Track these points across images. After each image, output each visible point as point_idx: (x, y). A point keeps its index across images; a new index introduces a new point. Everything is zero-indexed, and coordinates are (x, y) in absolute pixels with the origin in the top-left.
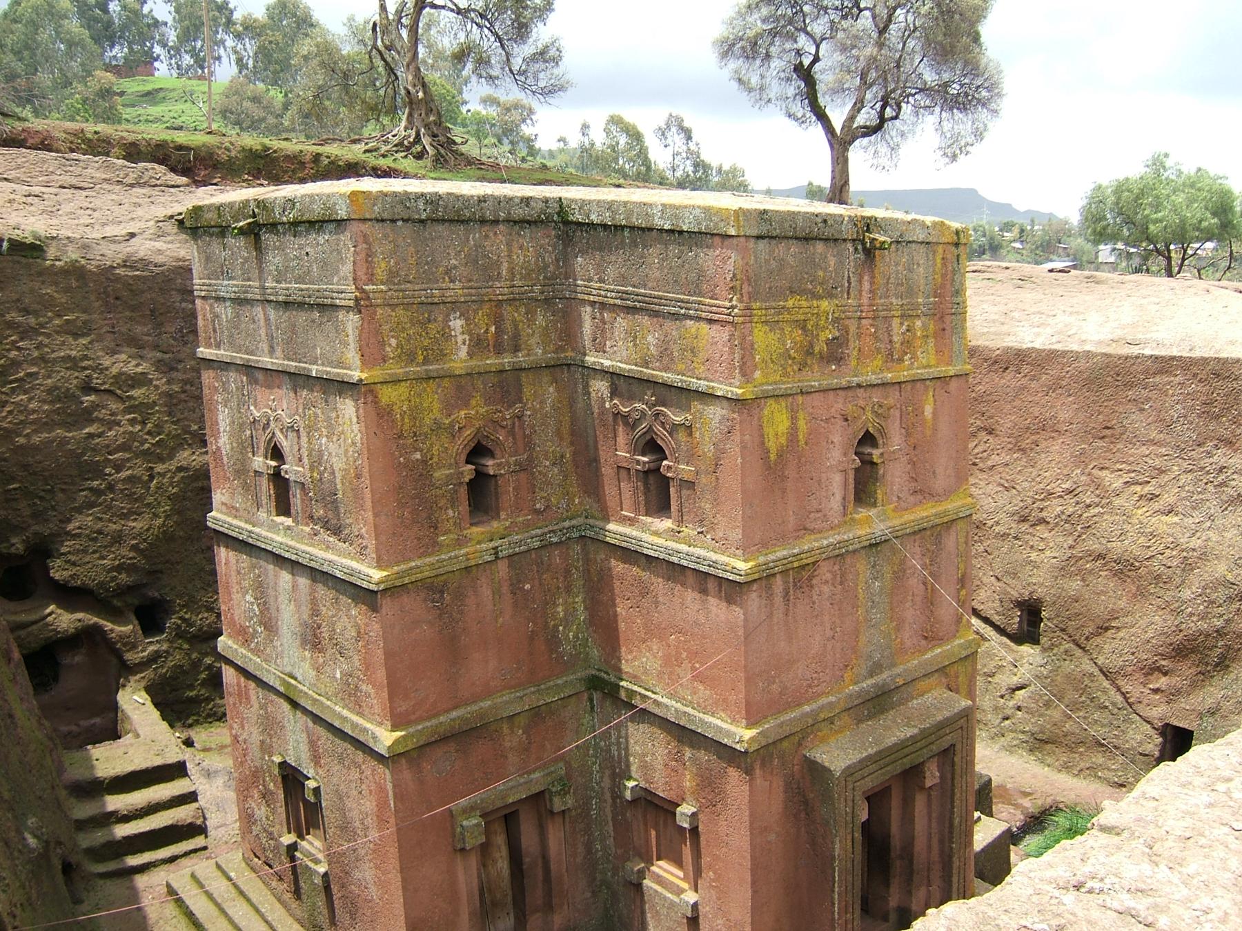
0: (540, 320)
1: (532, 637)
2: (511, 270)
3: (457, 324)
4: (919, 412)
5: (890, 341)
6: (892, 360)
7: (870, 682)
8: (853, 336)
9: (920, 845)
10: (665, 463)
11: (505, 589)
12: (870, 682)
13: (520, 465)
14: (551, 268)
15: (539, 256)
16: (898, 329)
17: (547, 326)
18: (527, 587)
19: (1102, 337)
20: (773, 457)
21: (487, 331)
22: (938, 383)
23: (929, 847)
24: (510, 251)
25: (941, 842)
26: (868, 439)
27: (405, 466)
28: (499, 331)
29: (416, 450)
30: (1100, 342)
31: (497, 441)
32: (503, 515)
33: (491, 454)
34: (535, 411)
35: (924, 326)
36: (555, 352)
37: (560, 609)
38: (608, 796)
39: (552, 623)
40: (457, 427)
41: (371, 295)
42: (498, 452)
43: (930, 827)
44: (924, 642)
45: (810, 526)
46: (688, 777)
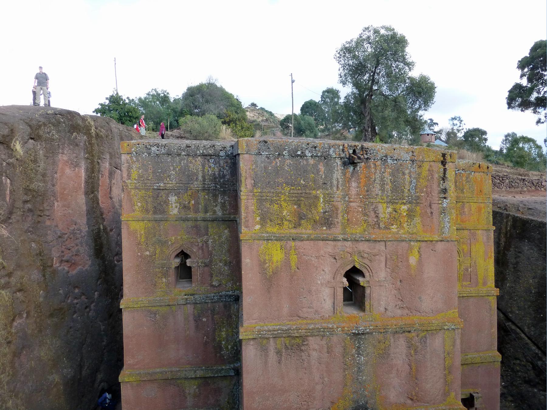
1: (206, 344)
2: (203, 177)
3: (173, 199)
5: (377, 216)
6: (379, 228)
8: (342, 212)
11: (191, 318)
13: (205, 263)
14: (228, 177)
15: (220, 170)
17: (225, 202)
18: (204, 320)
21: (189, 203)
22: (424, 244)
27: (141, 256)
28: (197, 203)
29: (147, 250)
31: (192, 251)
34: (214, 241)
36: (230, 214)
37: (223, 333)
39: (218, 339)
40: (170, 243)
41: (129, 185)
42: (192, 256)
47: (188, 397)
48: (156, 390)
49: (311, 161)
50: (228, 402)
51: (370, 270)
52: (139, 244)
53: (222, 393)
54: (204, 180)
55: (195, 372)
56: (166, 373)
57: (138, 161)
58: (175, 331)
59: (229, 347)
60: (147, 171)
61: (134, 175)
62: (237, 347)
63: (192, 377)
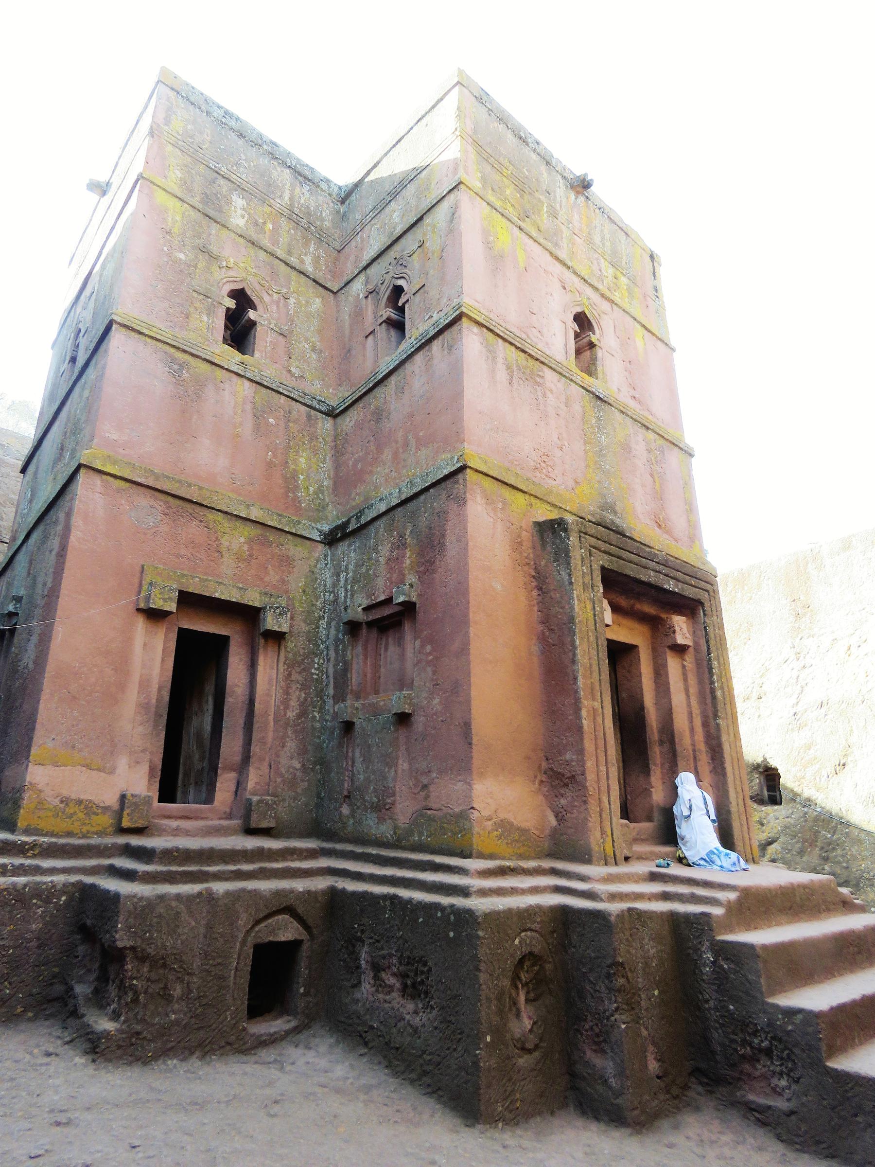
1: (270, 465)
9: (680, 722)
23: (692, 730)
25: (705, 724)
31: (261, 299)
38: (332, 654)
39: (293, 466)
43: (689, 705)
46: (408, 555)
47: (226, 555)
48: (159, 518)
50: (304, 591)
52: (169, 233)
53: (295, 570)
55: (248, 506)
56: (189, 485)
58: (215, 416)
59: (311, 489)
62: (323, 493)
63: (241, 515)
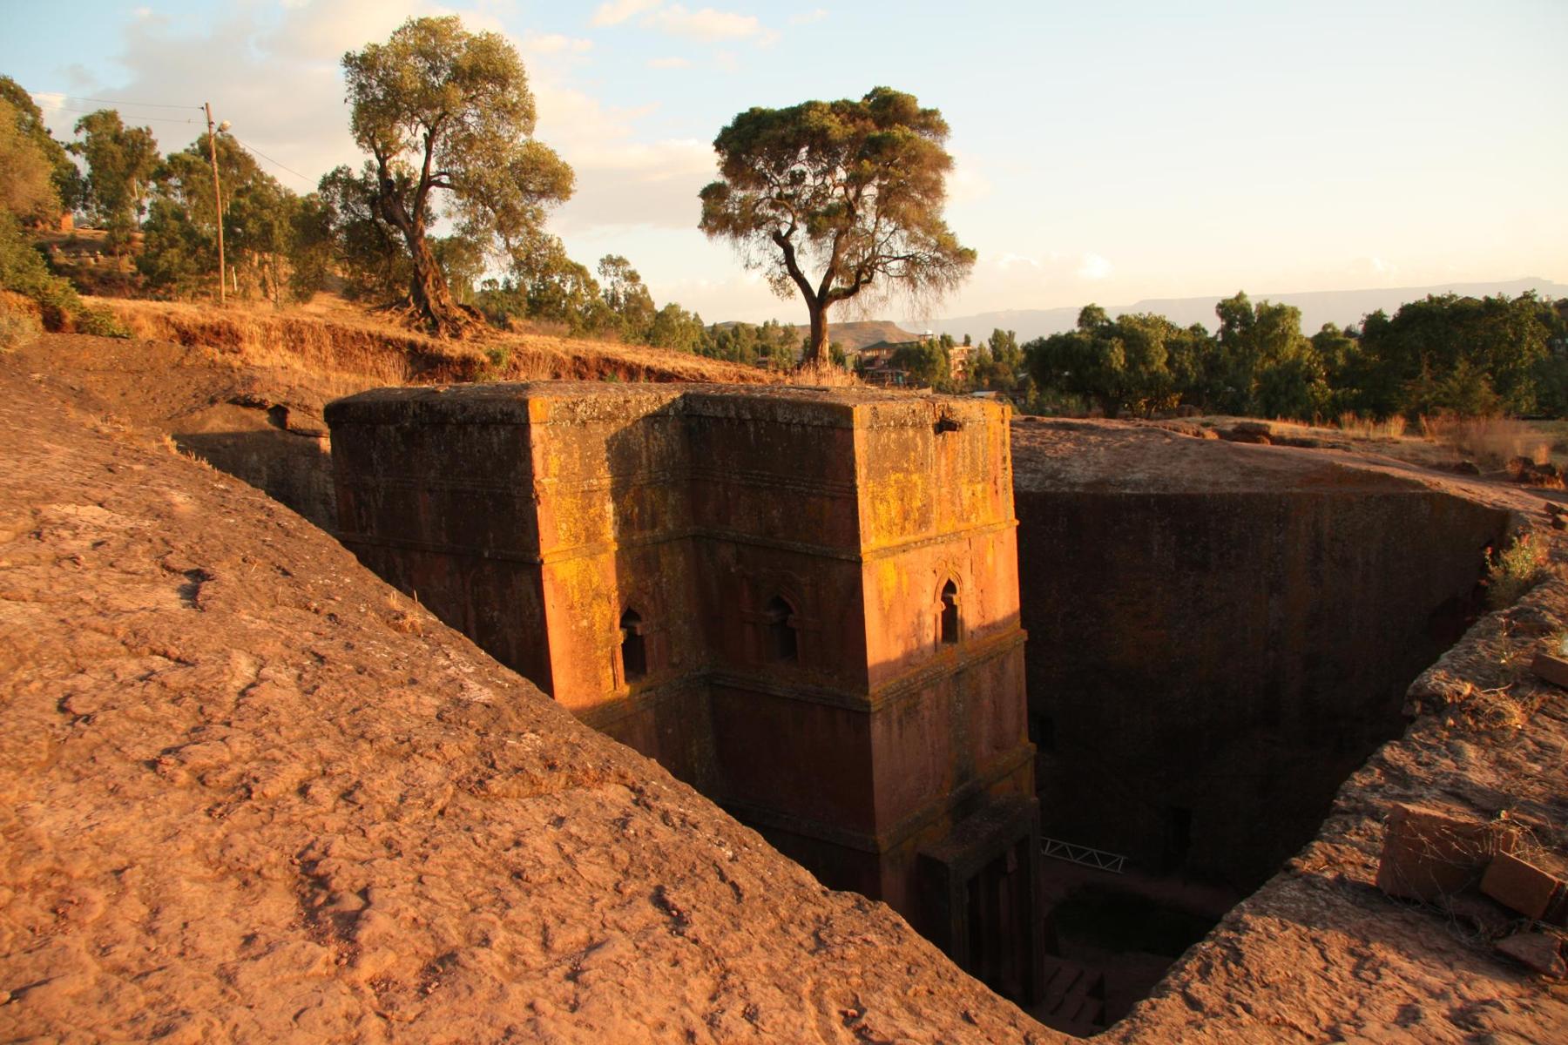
0: (671, 500)
2: (649, 459)
4: (983, 557)
7: (961, 788)
10: (791, 616)
12: (961, 788)
16: (966, 493)
19: (1087, 480)
20: (887, 608)
24: (647, 441)
26: (950, 588)
28: (642, 511)
29: (583, 618)
30: (1087, 485)
32: (649, 670)
33: (637, 617)
35: (984, 490)
37: (694, 748)
42: (643, 616)
44: (995, 752)
45: (912, 661)
49: (911, 433)
51: (960, 580)
54: (650, 465)
57: (556, 436)
60: (571, 455)
61: (554, 467)
